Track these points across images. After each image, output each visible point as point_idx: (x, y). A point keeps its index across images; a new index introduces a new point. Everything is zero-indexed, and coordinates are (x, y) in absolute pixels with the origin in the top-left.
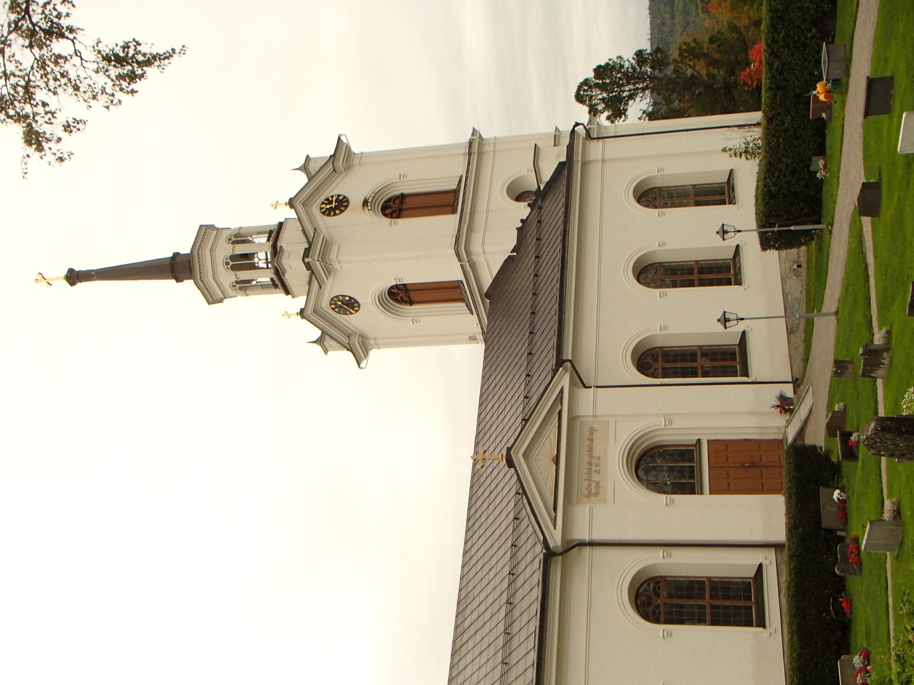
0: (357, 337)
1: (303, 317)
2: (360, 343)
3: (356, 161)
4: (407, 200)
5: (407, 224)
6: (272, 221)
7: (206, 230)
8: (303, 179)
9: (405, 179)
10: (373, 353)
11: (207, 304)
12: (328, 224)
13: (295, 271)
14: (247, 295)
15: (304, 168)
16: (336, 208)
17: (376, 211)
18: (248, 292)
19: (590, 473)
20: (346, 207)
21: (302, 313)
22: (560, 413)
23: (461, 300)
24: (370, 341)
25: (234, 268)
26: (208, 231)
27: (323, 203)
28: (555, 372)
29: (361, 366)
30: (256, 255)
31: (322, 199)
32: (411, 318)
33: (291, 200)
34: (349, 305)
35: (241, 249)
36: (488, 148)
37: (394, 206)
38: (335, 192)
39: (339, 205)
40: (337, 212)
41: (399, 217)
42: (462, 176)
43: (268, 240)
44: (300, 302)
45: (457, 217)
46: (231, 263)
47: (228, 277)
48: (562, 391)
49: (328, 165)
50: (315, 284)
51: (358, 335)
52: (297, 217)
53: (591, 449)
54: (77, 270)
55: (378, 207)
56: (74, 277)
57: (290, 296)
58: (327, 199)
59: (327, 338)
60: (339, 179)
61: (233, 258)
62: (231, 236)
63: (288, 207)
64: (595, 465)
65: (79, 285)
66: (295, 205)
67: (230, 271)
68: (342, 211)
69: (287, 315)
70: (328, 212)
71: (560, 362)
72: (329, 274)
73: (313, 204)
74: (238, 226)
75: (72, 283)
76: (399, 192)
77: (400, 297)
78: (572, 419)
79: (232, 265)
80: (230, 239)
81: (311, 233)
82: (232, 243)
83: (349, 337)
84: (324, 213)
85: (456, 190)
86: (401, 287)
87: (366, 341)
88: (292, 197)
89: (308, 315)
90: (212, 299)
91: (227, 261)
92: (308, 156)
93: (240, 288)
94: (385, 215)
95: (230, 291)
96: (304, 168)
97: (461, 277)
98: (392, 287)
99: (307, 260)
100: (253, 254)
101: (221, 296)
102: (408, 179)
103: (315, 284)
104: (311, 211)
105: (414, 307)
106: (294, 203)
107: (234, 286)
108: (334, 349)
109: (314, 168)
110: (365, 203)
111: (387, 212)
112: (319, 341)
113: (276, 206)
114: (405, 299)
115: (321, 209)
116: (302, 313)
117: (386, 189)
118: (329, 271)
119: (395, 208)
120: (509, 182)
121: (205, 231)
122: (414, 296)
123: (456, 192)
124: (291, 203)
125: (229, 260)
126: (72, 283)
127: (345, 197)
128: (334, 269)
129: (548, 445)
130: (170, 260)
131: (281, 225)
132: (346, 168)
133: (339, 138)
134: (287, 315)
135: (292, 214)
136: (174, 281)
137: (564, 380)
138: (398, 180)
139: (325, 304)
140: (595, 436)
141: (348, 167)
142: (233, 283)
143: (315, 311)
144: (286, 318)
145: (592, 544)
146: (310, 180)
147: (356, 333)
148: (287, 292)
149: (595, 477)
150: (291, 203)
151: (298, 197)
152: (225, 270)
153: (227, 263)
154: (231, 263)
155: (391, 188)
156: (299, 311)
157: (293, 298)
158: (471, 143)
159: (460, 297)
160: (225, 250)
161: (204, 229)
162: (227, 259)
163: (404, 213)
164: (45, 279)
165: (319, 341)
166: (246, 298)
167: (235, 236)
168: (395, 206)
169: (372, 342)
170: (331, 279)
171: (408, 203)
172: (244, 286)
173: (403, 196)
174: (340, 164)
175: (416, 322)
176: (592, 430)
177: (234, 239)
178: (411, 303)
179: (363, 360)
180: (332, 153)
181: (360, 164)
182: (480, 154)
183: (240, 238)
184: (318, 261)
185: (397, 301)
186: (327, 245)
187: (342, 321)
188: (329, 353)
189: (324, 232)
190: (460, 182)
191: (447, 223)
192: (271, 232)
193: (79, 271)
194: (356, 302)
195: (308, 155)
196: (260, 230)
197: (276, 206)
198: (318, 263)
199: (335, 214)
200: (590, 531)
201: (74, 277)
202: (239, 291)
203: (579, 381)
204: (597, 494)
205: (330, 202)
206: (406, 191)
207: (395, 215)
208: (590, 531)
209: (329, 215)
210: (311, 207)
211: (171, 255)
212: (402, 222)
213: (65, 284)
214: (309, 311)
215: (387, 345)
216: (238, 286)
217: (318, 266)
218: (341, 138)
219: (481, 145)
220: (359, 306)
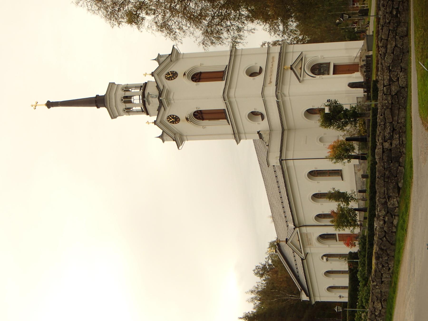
0: (178, 135)
2: (180, 137)
3: (181, 57)
5: (203, 85)
6: (141, 81)
7: (112, 85)
8: (156, 65)
9: (202, 66)
12: (169, 84)
13: (154, 103)
14: (129, 115)
15: (157, 59)
16: (173, 77)
17: (189, 79)
18: (130, 114)
20: (177, 77)
21: (155, 123)
23: (226, 118)
24: (184, 137)
25: (125, 102)
26: (113, 85)
27: (166, 74)
29: (179, 148)
30: (132, 98)
32: (202, 126)
33: (152, 73)
34: (176, 119)
35: (127, 94)
36: (239, 53)
37: (197, 77)
39: (173, 75)
40: (173, 78)
41: (199, 82)
42: (227, 65)
43: (140, 90)
44: (154, 118)
45: (224, 82)
46: (124, 100)
47: (122, 106)
51: (179, 134)
52: (155, 81)
54: (51, 101)
55: (190, 76)
56: (50, 105)
57: (149, 116)
58: (168, 73)
59: (165, 134)
60: (173, 65)
62: (123, 88)
63: (151, 76)
65: (52, 108)
66: (154, 75)
68: (174, 78)
69: (148, 123)
70: (168, 79)
72: (169, 105)
73: (162, 75)
74: (127, 83)
76: (199, 71)
77: (198, 117)
80: (123, 89)
81: (161, 88)
82: (124, 91)
83: (175, 134)
84: (167, 79)
85: (224, 71)
86: (199, 112)
87: (182, 137)
88: (153, 71)
89: (157, 123)
90: (113, 116)
91: (122, 99)
92: (159, 54)
93: (127, 112)
94: (193, 81)
96: (157, 59)
98: (195, 112)
99: (161, 98)
100: (132, 96)
101: (117, 114)
102: (204, 65)
103: (162, 109)
104: (161, 78)
106: (154, 74)
107: (124, 110)
108: (167, 140)
109: (162, 60)
111: (194, 80)
112: (161, 137)
113: (145, 75)
114: (201, 117)
115: (165, 77)
116: (155, 123)
117: (193, 70)
118: (169, 104)
119: (197, 78)
121: (111, 85)
122: (205, 116)
123: (223, 72)
124: (152, 74)
125: (123, 99)
127: (176, 72)
128: (171, 103)
131: (146, 83)
132: (176, 60)
134: (148, 123)
135: (152, 79)
138: (200, 66)
141: (177, 59)
142: (124, 109)
144: (147, 124)
146: (160, 64)
147: (178, 133)
148: (148, 114)
150: (152, 74)
151: (155, 72)
152: (121, 103)
154: (124, 100)
155: (195, 70)
156: (153, 122)
157: (150, 116)
158: (231, 51)
160: (121, 94)
161: (111, 84)
162: (122, 98)
163: (200, 80)
165: (161, 137)
166: (128, 116)
167: (125, 88)
168: (197, 77)
169: (185, 137)
171: (202, 76)
172: (128, 111)
173: (201, 73)
175: (205, 128)
177: (125, 89)
178: (203, 119)
179: (180, 146)
180: (170, 53)
181: (183, 58)
182: (235, 56)
183: (127, 88)
184: (165, 99)
186: (168, 92)
188: (165, 142)
189: (167, 87)
190: (226, 67)
191: (220, 85)
192: (141, 87)
193: (52, 102)
194: (178, 118)
195: (159, 54)
196: (136, 86)
197: (145, 75)
198: (164, 100)
199: (172, 79)
201: (50, 105)
202: (126, 113)
205: (170, 74)
206: (203, 70)
209: (169, 80)
210: (161, 76)
211: (95, 96)
212: (201, 83)
216: (126, 110)
217: (164, 101)
218: (174, 46)
219: (235, 52)
220: (179, 120)
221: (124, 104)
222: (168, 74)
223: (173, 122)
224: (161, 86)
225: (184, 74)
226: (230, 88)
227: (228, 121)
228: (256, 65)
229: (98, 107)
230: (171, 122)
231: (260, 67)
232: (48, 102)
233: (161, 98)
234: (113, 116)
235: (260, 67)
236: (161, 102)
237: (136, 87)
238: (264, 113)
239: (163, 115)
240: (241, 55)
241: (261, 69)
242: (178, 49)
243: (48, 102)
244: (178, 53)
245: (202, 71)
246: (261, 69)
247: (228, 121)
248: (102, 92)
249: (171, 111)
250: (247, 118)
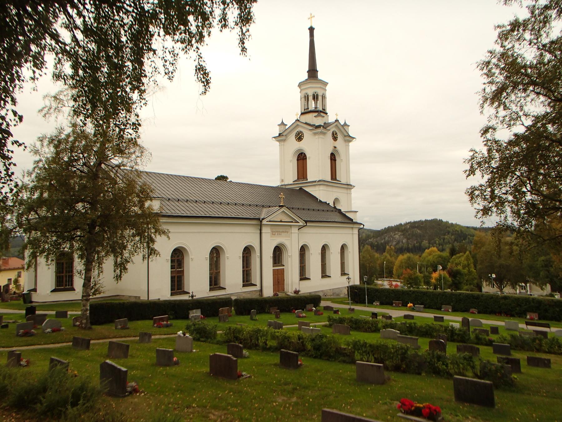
10: (278, 143)
15: (345, 124)
16: (334, 136)
18: (303, 99)
19: (278, 232)
22: (292, 222)
23: (298, 178)
25: (314, 95)
28: (304, 221)
31: (337, 132)
34: (299, 137)
36: (349, 191)
38: (339, 136)
47: (310, 93)
48: (298, 222)
53: (283, 232)
56: (311, 30)
61: (317, 95)
64: (279, 233)
65: (309, 31)
70: (333, 134)
71: (306, 222)
76: (337, 159)
78: (291, 226)
95: (304, 92)
96: (345, 124)
97: (309, 180)
101: (302, 88)
109: (346, 127)
110: (335, 147)
112: (283, 124)
114: (299, 158)
118: (315, 134)
121: (326, 84)
122: (301, 162)
123: (336, 179)
126: (309, 29)
129: (285, 218)
137: (301, 223)
139: (300, 129)
140: (286, 233)
141: (345, 141)
145: (261, 233)
146: (342, 126)
149: (277, 233)
153: (315, 93)
169: (282, 143)
171: (333, 162)
174: (348, 138)
176: (288, 232)
178: (298, 160)
182: (347, 188)
185: (300, 154)
186: (324, 134)
187: (292, 134)
188: (278, 126)
192: (324, 110)
194: (300, 141)
200: (265, 233)
201: (311, 30)
203: (300, 228)
204: (273, 234)
208: (265, 233)
213: (309, 26)
215: (281, 149)
217: (319, 130)
220: (298, 141)
222: (336, 134)
223: (296, 136)
229: (308, 72)
232: (314, 29)
233: (322, 127)
236: (319, 127)
237: (324, 105)
239: (304, 128)
240: (347, 193)
243: (314, 29)
244: (350, 141)
248: (320, 76)
249: (307, 134)
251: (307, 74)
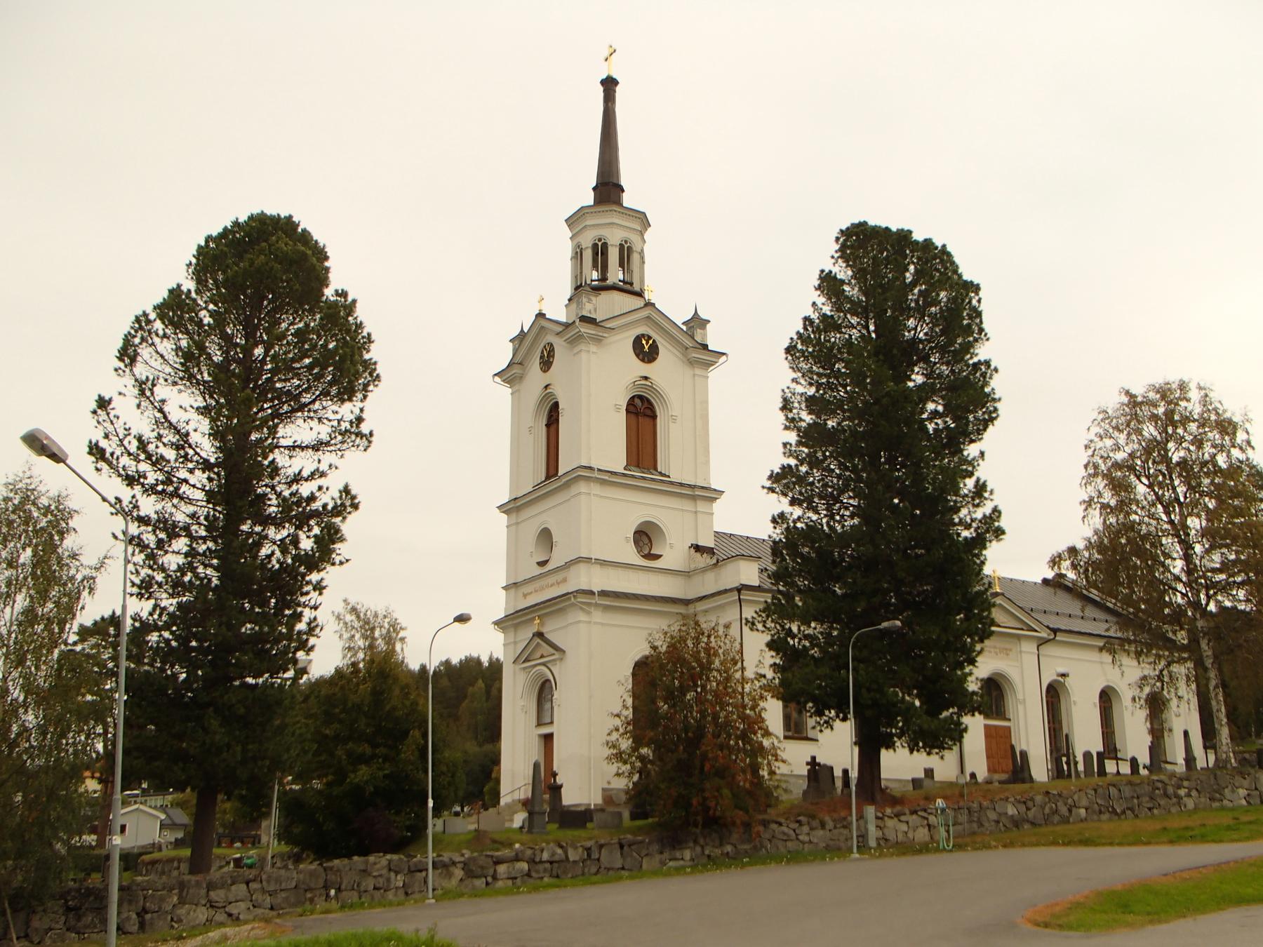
1: (536, 316)
3: (698, 371)
4: (648, 420)
8: (680, 316)
11: (566, 218)
21: (541, 315)
23: (548, 477)
25: (595, 246)
31: (654, 336)
33: (653, 305)
34: (546, 364)
36: (701, 507)
39: (646, 351)
42: (669, 477)
43: (620, 281)
46: (600, 244)
47: (587, 240)
49: (693, 342)
50: (560, 329)
56: (609, 84)
61: (605, 246)
65: (601, 89)
67: (592, 243)
75: (603, 82)
76: (658, 414)
79: (598, 245)
80: (626, 242)
92: (709, 321)
93: (577, 252)
102: (671, 424)
105: (544, 428)
106: (649, 307)
116: (541, 315)
120: (661, 526)
122: (553, 428)
126: (603, 82)
130: (615, 182)
133: (724, 354)
136: (595, 184)
139: (550, 338)
141: (692, 363)
143: (542, 327)
144: (539, 298)
153: (600, 240)
154: (600, 244)
156: (543, 312)
157: (566, 306)
159: (551, 474)
160: (614, 238)
163: (633, 417)
164: (611, 54)
170: (564, 343)
173: (654, 417)
177: (626, 246)
178: (548, 426)
181: (694, 375)
182: (694, 498)
189: (613, 338)
195: (709, 321)
201: (609, 84)
206: (660, 422)
207: (632, 409)
212: (622, 416)
214: (543, 323)
216: (578, 250)
221: (590, 245)
224: (614, 324)
225: (646, 378)
226: (601, 484)
227: (544, 481)
228: (668, 546)
229: (594, 189)
230: (542, 352)
231: (661, 556)
234: (571, 221)
235: (661, 556)
238: (550, 567)
240: (696, 512)
241: (658, 557)
242: (717, 364)
244: (708, 365)
245: (658, 418)
246: (658, 557)
247: (544, 481)
248: (628, 200)
250: (543, 527)
251: (592, 193)
